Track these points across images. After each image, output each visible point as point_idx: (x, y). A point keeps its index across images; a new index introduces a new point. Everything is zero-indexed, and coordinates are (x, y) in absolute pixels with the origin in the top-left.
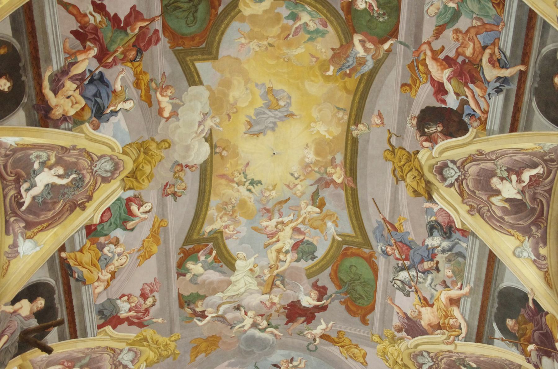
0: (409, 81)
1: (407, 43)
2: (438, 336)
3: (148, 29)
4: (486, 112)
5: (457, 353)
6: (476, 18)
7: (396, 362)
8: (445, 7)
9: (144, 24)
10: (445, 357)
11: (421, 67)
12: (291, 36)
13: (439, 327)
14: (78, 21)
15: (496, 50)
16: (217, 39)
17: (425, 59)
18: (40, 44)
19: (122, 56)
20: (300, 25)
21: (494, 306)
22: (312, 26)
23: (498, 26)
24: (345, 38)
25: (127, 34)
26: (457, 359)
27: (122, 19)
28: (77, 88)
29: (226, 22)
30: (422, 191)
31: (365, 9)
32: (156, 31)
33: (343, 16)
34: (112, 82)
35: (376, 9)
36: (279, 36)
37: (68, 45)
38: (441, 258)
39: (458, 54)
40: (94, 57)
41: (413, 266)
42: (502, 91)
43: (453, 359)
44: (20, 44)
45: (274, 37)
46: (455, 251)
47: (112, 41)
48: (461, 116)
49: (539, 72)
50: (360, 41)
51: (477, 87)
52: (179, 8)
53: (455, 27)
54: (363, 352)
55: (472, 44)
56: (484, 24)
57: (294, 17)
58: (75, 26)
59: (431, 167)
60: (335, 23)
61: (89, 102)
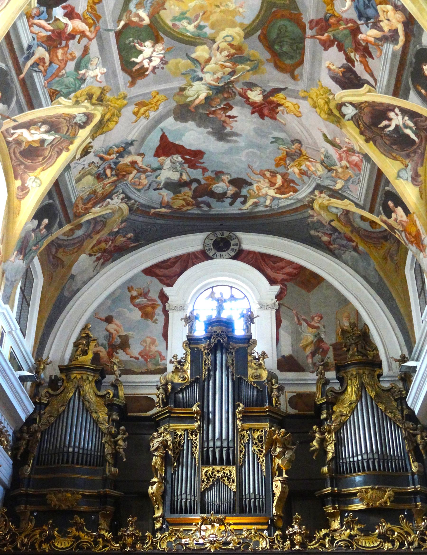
0: (96, 7)
1: (106, 32)
3: (317, 33)
4: (30, 26)
6: (64, 75)
8: (86, 68)
9: (319, 37)
11: (92, 21)
12: (201, 14)
14: (367, 62)
15: (42, 69)
16: (263, 12)
17: (89, 28)
18: (396, 69)
19: (340, 22)
20: (194, 22)
22: (185, 23)
23: (48, 83)
24: (156, 19)
25: (334, 35)
27: (335, 47)
28: (381, 21)
29: (255, 24)
31: (144, 41)
32: (311, 28)
33: (160, 33)
34: (353, 8)
35: (137, 45)
36: (211, 13)
37: (378, 53)
39: (67, 46)
40: (361, 33)
42: (27, 50)
44: (408, 83)
45: (215, 12)
47: (346, 36)
48: (47, 9)
49: (12, 85)
50: (143, 20)
51: (44, 36)
52: (291, 39)
53: (76, 60)
55: (60, 58)
56: (57, 76)
57: (199, 27)
58: (369, 60)
60: (166, 28)
61: (374, 5)
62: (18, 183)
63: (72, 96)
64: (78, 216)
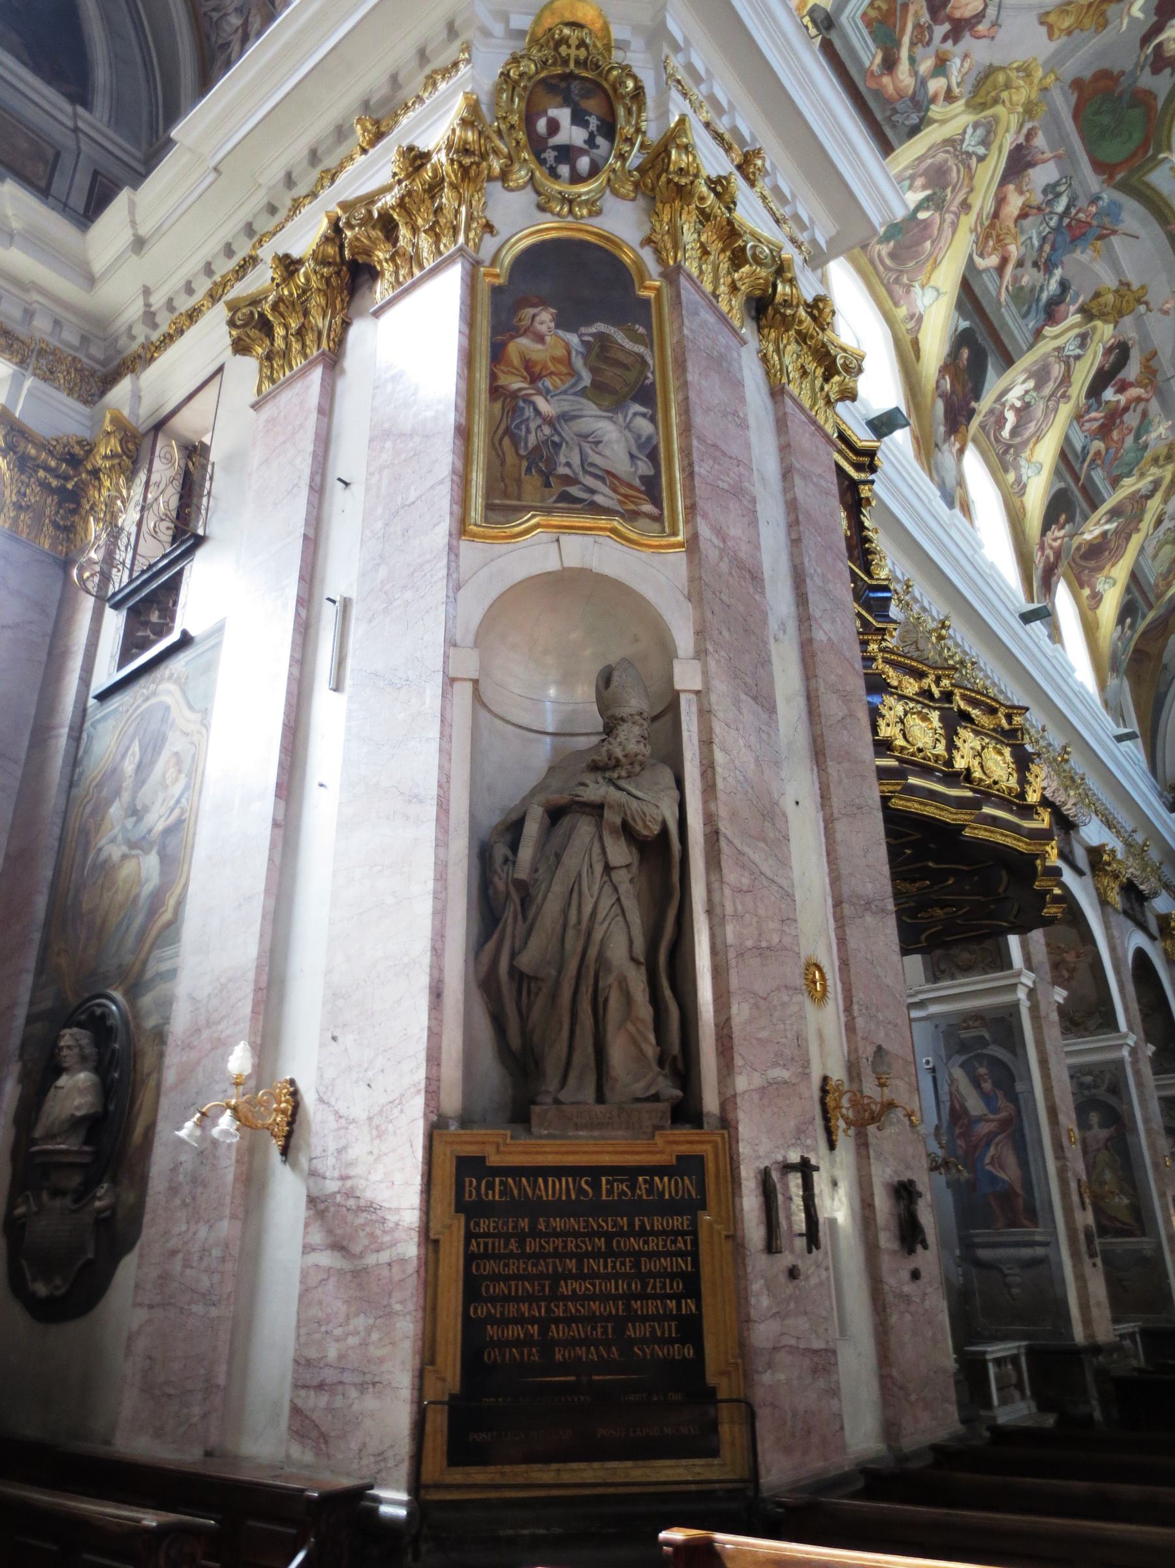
0: (1152, 363)
2: (989, 206)
5: (958, 217)
7: (1008, 86)
8: (1147, 432)
10: (959, 177)
13: (996, 215)
21: (983, 339)
26: (944, 200)
30: (1094, 304)
38: (1039, 276)
41: (1057, 230)
43: (949, 189)
46: (1034, 306)
54: (1057, 33)
59: (1094, 329)
62: (1086, 592)
63: (1135, 471)
64: (1159, 596)
